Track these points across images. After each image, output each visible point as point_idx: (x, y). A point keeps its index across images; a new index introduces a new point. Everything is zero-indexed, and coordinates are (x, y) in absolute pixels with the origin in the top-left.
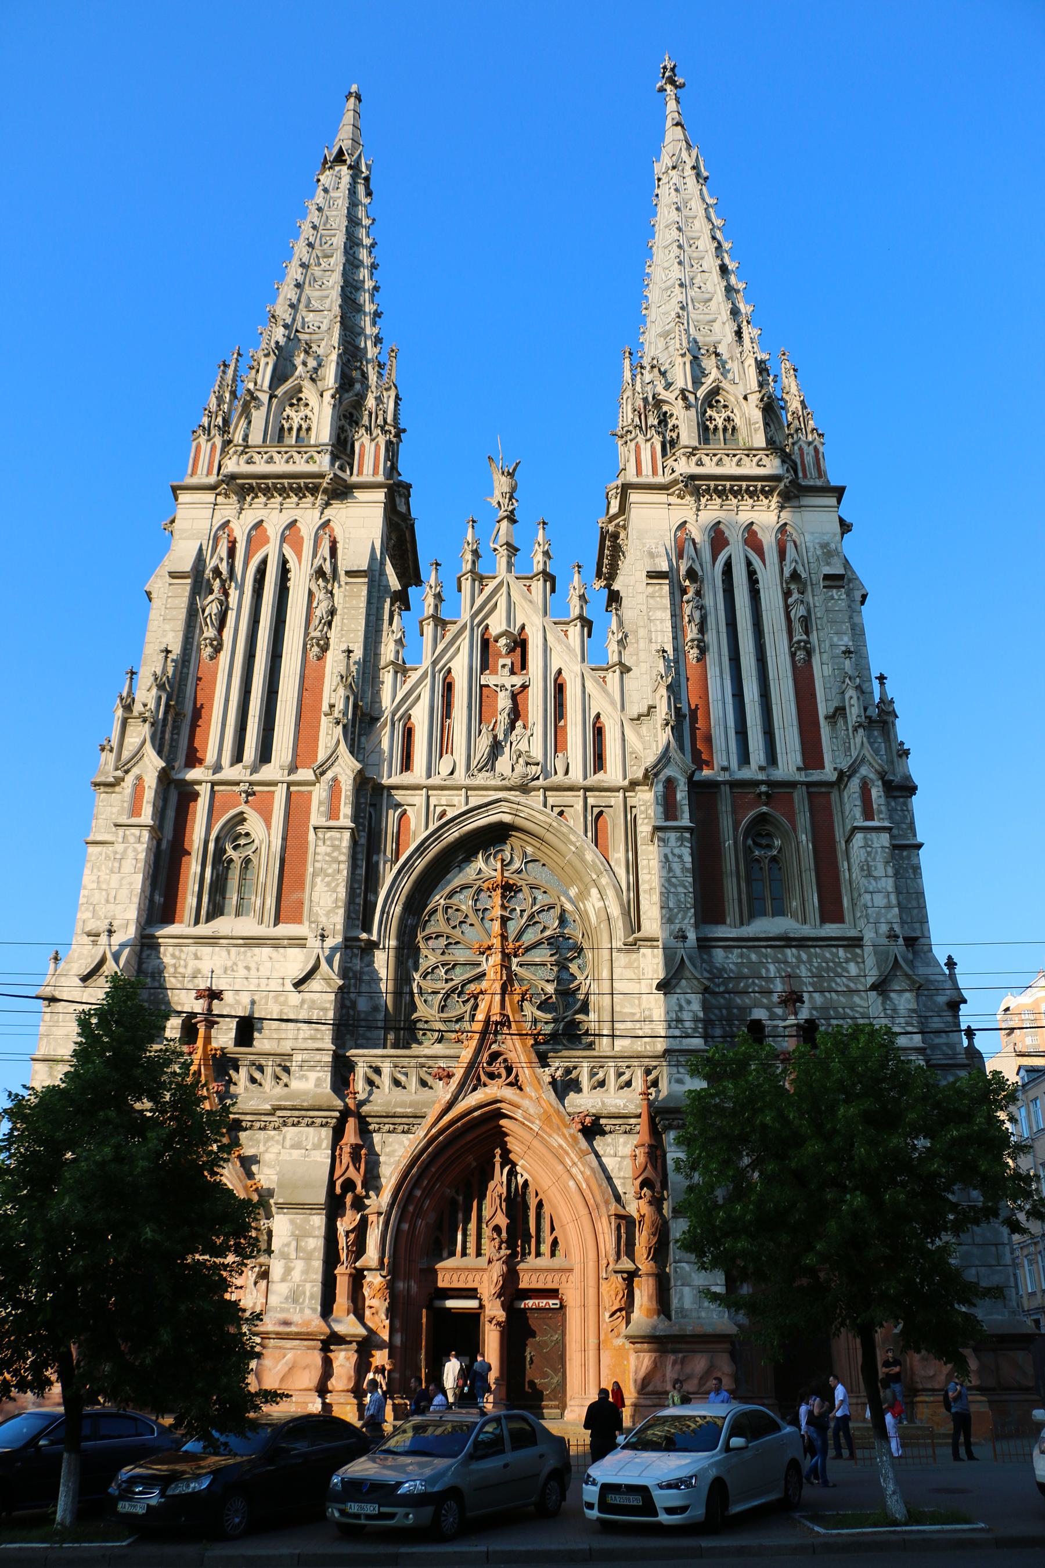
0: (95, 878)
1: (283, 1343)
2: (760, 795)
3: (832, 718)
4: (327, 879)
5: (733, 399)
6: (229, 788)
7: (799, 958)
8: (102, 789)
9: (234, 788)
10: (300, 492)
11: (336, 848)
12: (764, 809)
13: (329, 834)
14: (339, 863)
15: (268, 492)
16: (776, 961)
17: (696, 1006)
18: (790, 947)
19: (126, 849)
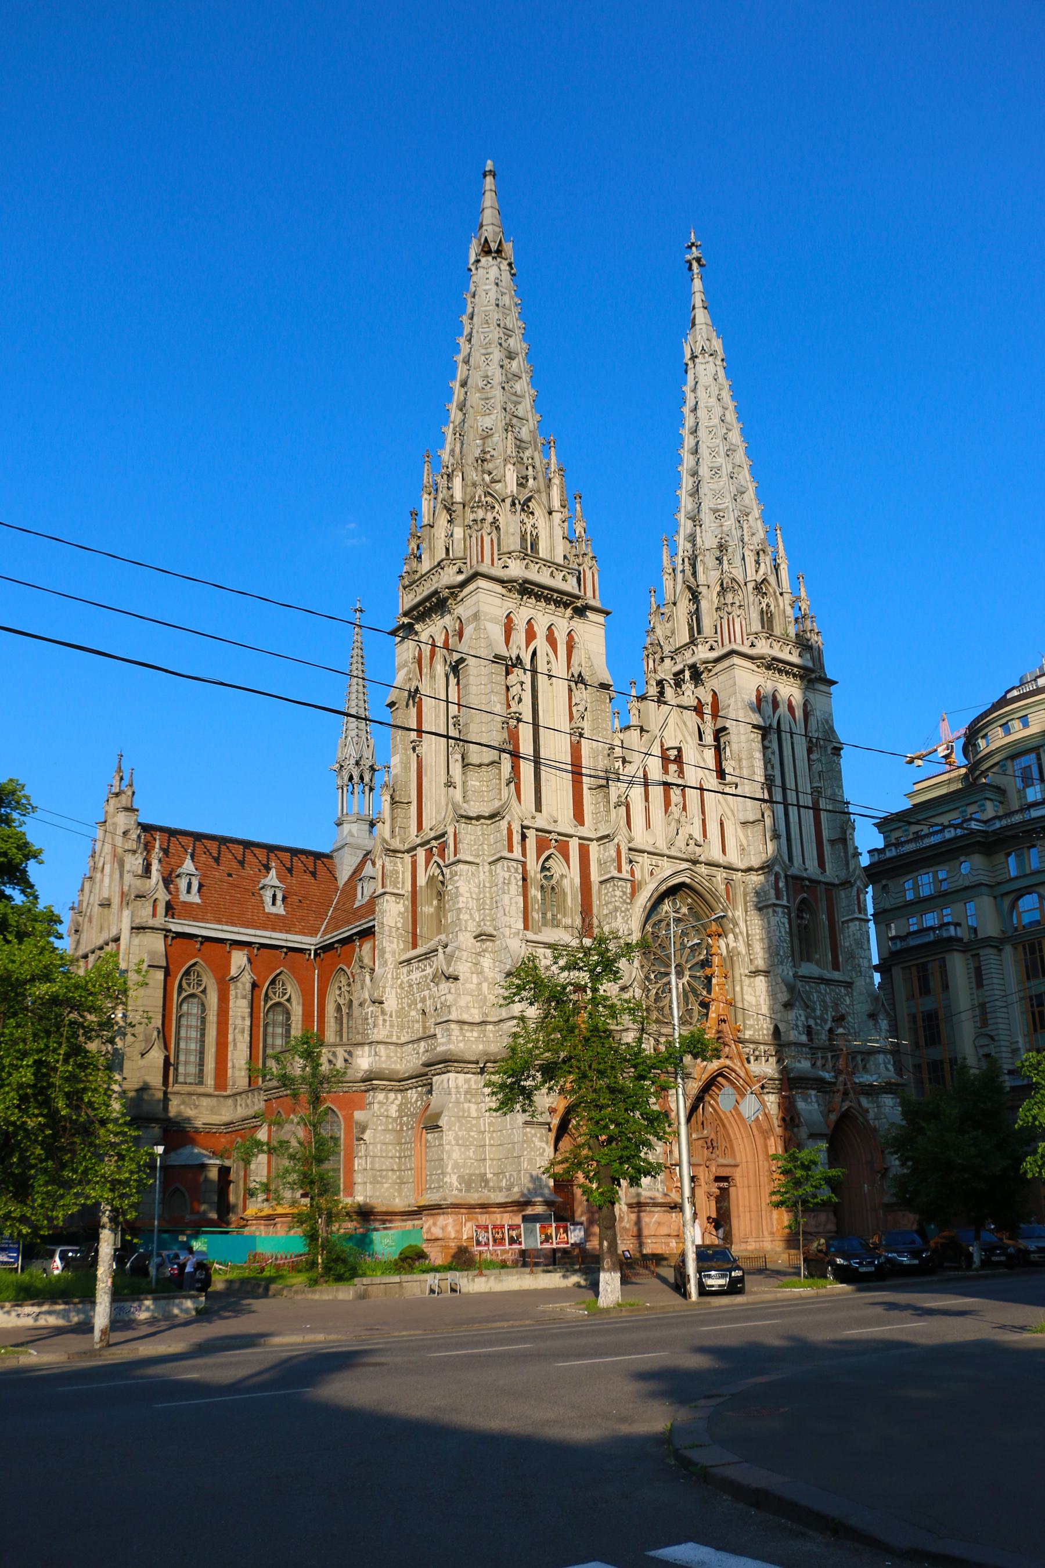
0: (467, 889)
1: (653, 1209)
2: (803, 886)
3: (832, 842)
4: (623, 914)
5: (771, 591)
6: (544, 834)
7: (825, 990)
8: (464, 820)
9: (547, 835)
10: (558, 603)
11: (625, 893)
12: (805, 895)
13: (620, 883)
14: (627, 903)
15: (538, 597)
16: (817, 992)
17: (803, 1018)
18: (822, 983)
19: (510, 876)
